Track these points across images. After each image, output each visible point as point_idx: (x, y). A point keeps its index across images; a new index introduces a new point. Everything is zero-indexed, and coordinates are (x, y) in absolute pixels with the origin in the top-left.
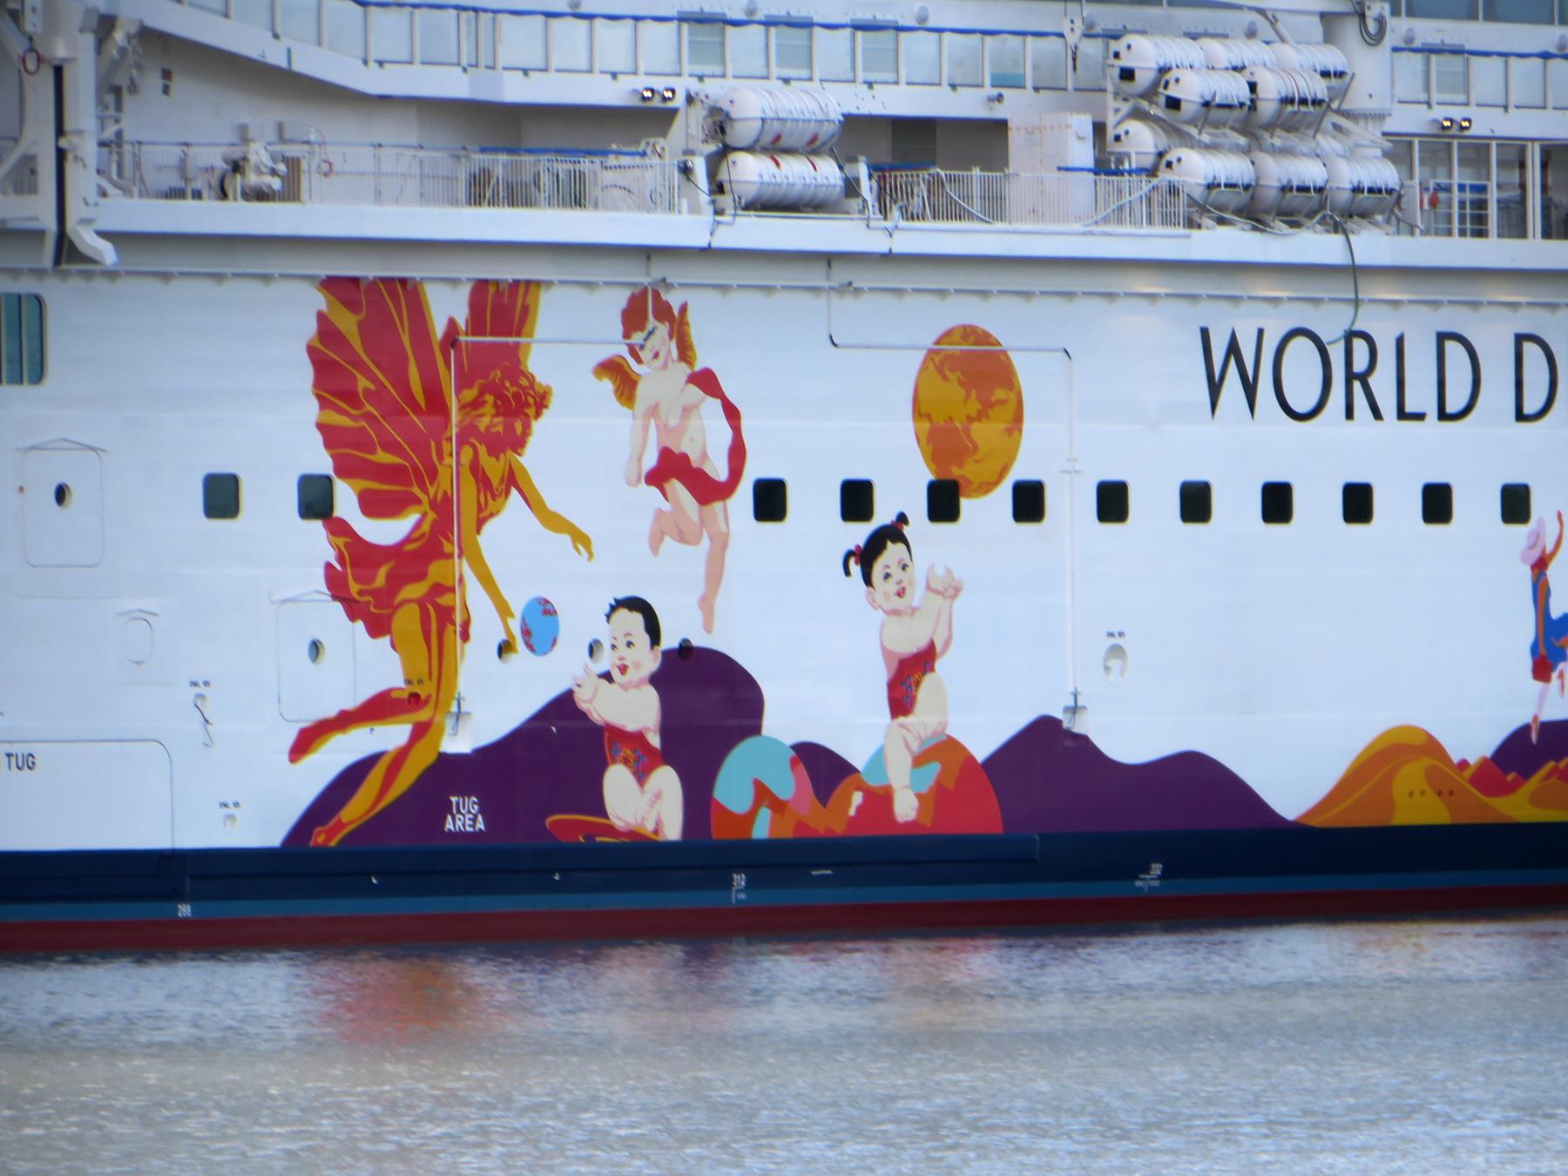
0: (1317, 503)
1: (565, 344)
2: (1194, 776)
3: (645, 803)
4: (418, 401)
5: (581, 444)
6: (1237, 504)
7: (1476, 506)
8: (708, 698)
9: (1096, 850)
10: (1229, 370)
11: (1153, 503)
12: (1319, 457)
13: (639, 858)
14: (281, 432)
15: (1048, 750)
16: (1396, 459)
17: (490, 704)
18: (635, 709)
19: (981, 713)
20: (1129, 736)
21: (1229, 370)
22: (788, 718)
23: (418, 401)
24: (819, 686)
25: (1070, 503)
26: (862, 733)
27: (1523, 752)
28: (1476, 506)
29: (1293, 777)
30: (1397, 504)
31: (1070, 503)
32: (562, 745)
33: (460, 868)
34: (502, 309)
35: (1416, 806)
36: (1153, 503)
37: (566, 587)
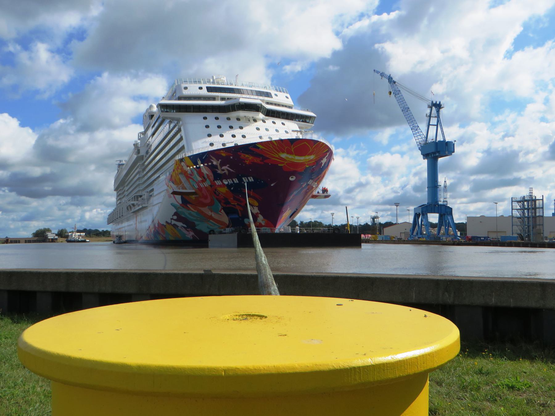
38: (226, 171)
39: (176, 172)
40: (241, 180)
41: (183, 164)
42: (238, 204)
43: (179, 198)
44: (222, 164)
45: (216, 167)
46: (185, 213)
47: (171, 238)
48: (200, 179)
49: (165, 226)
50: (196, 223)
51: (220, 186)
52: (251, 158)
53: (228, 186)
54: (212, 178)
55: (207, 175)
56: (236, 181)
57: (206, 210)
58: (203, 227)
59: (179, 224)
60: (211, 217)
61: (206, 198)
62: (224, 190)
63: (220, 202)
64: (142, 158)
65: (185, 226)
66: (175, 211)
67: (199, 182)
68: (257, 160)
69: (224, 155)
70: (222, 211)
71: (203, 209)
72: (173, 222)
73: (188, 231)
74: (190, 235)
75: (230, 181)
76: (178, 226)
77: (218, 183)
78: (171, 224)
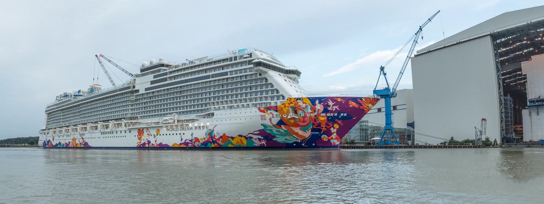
0: (171, 134)
1: (145, 131)
2: (166, 145)
3: (147, 146)
4: (141, 132)
5: (145, 134)
6: (168, 135)
7: (178, 134)
8: (149, 142)
9: (162, 147)
10: (168, 130)
11: (165, 135)
12: (171, 133)
13: (147, 148)
14: (137, 134)
15: (161, 144)
16: (175, 133)
17: (142, 142)
18: (147, 142)
19: (158, 143)
20: (164, 143)
21: (168, 130)
22: (152, 143)
23: (141, 132)
24: (153, 142)
25: (162, 135)
26: (154, 143)
27: (181, 144)
28: (178, 134)
29: (171, 145)
30: (175, 134)
31: (162, 135)
32: (144, 144)
33: (142, 147)
34: (143, 129)
35: (176, 146)
36: (165, 135)
37: (145, 138)
38: (334, 109)
39: (287, 105)
40: (339, 114)
41: (298, 101)
42: (326, 127)
43: (275, 121)
44: (333, 106)
45: (329, 106)
46: (274, 130)
47: (230, 146)
48: (310, 111)
49: (233, 138)
50: (277, 136)
51: (323, 116)
52: (354, 104)
53: (328, 117)
54: (320, 112)
55: (319, 110)
56: (336, 115)
57: (297, 130)
58: (280, 139)
59: (255, 137)
60: (297, 134)
61: (304, 121)
62: (322, 119)
63: (313, 124)
64: (137, 91)
65: (262, 138)
66: (262, 128)
67: (308, 113)
68: (357, 106)
69: (339, 100)
70: (310, 130)
71: (293, 128)
72: (250, 135)
73: (260, 141)
74: (257, 143)
75: (332, 114)
76: (251, 138)
77: (324, 115)
78: (244, 137)
